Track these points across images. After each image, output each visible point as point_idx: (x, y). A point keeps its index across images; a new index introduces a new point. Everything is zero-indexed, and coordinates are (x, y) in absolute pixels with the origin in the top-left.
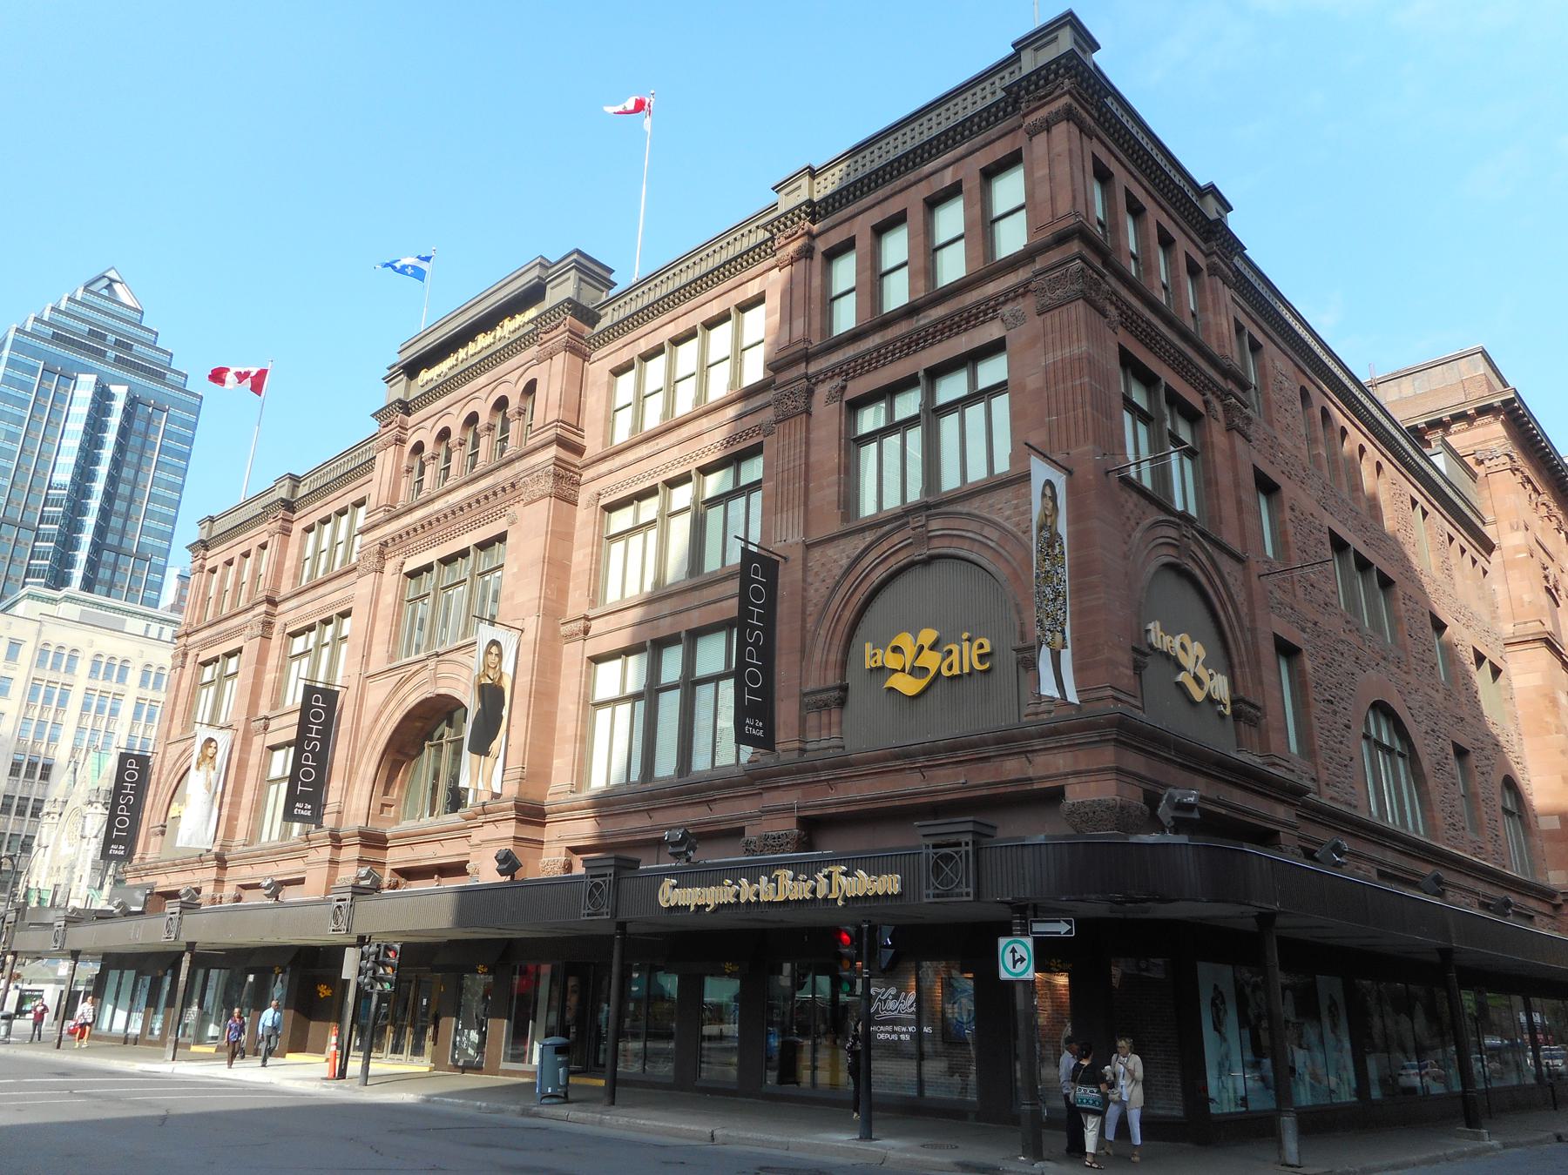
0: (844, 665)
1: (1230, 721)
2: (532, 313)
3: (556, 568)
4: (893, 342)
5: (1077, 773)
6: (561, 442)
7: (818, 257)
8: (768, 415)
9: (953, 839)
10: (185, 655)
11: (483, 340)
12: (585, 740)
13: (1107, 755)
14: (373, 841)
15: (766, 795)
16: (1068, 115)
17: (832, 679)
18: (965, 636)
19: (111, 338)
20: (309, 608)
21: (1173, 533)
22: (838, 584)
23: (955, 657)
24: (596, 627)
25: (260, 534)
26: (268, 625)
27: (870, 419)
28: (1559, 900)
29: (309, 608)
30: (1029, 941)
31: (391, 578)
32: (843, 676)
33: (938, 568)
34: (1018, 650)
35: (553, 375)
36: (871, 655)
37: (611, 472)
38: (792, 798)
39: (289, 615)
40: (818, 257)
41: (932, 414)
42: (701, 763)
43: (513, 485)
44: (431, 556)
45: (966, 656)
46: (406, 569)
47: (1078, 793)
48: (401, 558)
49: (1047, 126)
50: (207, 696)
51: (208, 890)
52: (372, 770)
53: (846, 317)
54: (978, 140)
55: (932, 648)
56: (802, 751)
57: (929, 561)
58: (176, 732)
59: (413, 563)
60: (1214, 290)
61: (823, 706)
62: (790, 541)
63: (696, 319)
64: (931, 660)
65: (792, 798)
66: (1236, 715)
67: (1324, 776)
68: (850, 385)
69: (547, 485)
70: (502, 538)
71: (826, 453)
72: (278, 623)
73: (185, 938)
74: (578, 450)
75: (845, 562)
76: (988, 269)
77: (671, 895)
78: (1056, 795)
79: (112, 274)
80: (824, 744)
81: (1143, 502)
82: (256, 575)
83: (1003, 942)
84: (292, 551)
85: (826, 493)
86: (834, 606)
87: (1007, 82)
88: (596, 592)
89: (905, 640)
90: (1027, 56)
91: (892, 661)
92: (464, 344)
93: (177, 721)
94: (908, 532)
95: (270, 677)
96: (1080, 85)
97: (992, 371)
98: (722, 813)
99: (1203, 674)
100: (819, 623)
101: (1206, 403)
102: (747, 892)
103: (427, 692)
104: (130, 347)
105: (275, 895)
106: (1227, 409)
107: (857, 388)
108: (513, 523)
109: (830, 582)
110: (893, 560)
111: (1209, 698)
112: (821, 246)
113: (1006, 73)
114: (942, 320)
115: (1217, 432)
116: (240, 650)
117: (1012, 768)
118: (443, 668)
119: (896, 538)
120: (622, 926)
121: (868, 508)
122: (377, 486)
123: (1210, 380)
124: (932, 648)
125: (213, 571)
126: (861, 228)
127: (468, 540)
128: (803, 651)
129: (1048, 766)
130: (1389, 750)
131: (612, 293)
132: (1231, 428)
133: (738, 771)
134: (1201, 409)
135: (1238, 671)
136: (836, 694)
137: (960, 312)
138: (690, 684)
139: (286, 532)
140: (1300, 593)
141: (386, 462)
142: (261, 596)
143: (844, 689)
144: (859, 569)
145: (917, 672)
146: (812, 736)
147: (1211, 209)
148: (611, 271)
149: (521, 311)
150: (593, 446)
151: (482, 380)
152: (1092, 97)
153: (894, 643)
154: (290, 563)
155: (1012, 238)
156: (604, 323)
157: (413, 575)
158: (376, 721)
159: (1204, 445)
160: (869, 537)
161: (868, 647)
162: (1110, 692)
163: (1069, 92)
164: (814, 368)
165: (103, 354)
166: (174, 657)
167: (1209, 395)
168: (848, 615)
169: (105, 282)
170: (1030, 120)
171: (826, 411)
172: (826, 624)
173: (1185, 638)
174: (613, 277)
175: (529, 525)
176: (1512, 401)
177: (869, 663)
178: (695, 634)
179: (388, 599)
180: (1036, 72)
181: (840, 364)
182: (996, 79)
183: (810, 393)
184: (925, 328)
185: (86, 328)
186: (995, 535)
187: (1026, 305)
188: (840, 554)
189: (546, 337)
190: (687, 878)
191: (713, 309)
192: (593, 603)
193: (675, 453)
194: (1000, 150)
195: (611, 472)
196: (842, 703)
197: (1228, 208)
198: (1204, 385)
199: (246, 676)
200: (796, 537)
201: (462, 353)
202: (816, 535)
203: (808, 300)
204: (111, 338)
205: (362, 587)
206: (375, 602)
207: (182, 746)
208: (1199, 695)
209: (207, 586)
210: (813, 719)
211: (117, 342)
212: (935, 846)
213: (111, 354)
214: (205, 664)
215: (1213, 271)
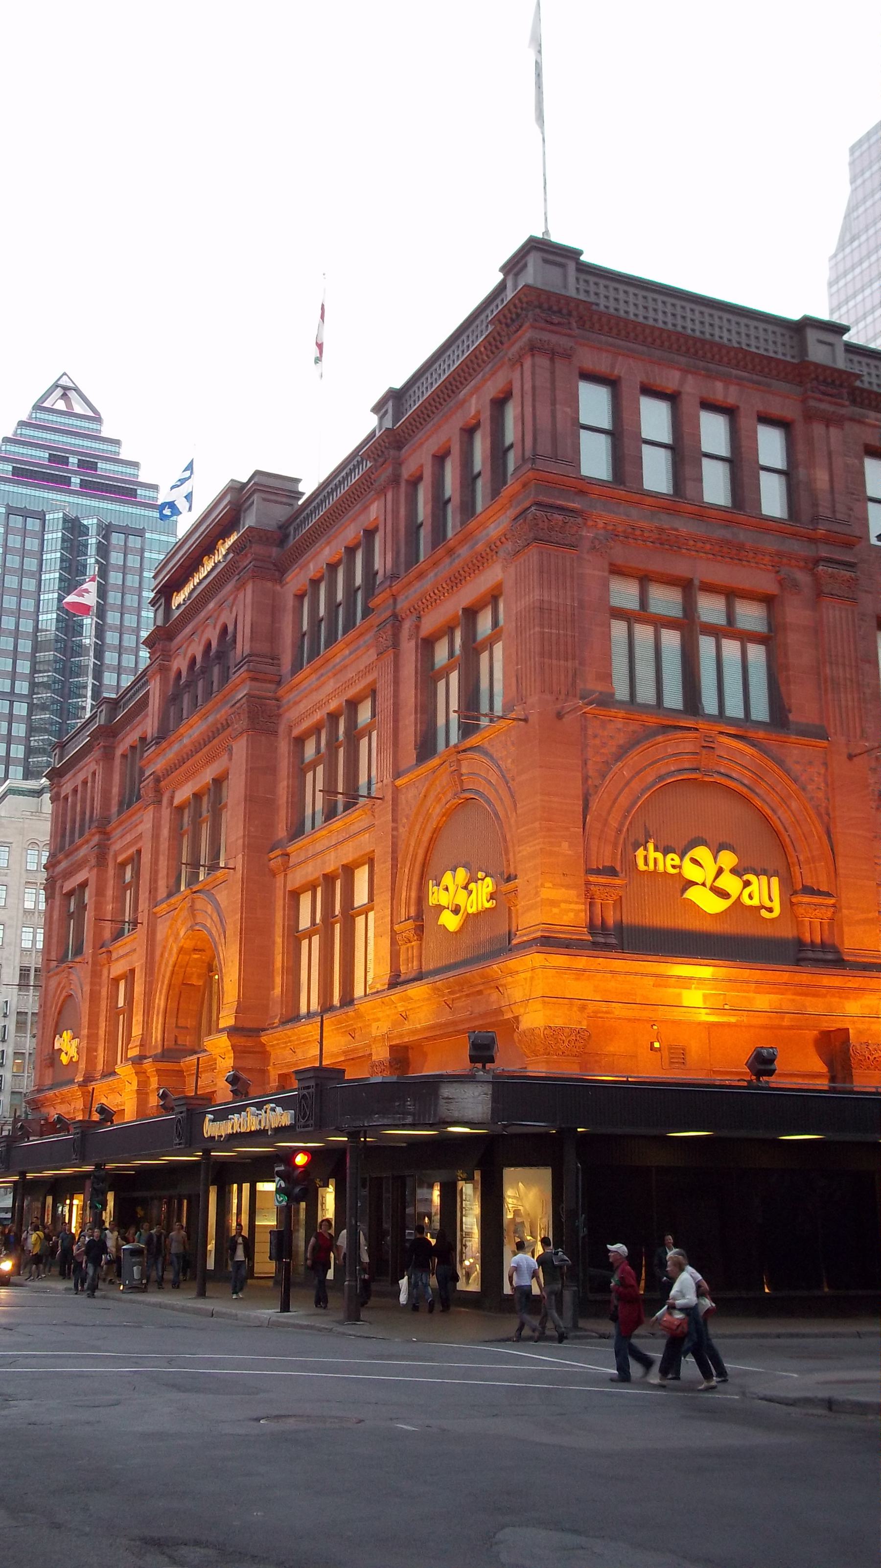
2: (234, 537)
16: (533, 349)
19: (74, 460)
46: (176, 802)
62: (385, 782)
69: (241, 724)
79: (64, 381)
104: (94, 466)
113: (493, 306)
128: (393, 890)
165: (67, 481)
169: (59, 392)
174: (301, 488)
204: (74, 460)
206: (156, 836)
213: (76, 480)
215: (809, 417)
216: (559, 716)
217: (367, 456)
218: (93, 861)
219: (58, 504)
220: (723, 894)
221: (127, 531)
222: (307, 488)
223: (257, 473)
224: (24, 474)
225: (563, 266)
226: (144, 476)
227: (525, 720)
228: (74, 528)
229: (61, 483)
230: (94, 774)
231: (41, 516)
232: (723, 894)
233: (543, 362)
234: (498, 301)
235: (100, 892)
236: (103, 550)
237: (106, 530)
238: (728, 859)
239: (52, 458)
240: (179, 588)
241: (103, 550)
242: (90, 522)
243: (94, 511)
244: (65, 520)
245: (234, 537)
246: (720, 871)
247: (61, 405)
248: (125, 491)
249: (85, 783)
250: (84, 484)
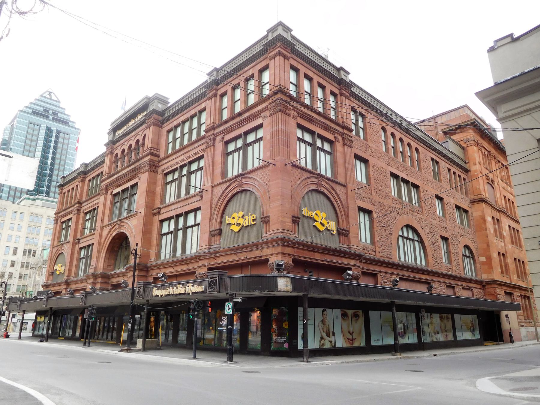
0: (221, 222)
1: (337, 236)
2: (145, 113)
3: (150, 193)
4: (235, 124)
5: (272, 254)
6: (151, 154)
7: (218, 96)
8: (204, 146)
9: (214, 276)
10: (57, 220)
11: (133, 122)
12: (159, 245)
13: (279, 249)
14: (106, 277)
15: (200, 262)
16: (280, 54)
17: (218, 228)
18: (250, 214)
19: (51, 112)
20: (90, 205)
21: (315, 180)
22: (220, 198)
23: (247, 220)
24: (162, 211)
25: (76, 183)
26: (79, 210)
28: (484, 284)
29: (90, 205)
30: (232, 304)
31: (109, 197)
32: (220, 226)
33: (245, 193)
34: (261, 218)
35: (150, 133)
36: (227, 219)
37: (166, 163)
38: (206, 262)
39: (86, 207)
40: (218, 96)
41: (246, 145)
42: (188, 252)
43: (139, 167)
44: (119, 189)
45: (249, 220)
46: (113, 193)
47: (273, 260)
48: (111, 190)
49: (274, 57)
50: (64, 232)
51: (64, 292)
52: (104, 255)
53: (225, 115)
54: (258, 61)
55: (242, 217)
56: (209, 248)
57: (243, 191)
58: (55, 244)
59: (115, 191)
60: (341, 101)
61: (215, 235)
63: (188, 115)
64: (241, 221)
65: (206, 262)
66: (339, 233)
67: (378, 249)
68: (225, 137)
69: (147, 168)
70: (137, 184)
71: (219, 158)
73: (49, 307)
74: (158, 156)
75: (222, 192)
76: (262, 100)
77: (156, 292)
78: (267, 261)
79: (50, 91)
80: (215, 246)
81: (303, 171)
82: (76, 194)
83: (226, 304)
84: (86, 187)
85: (218, 171)
86: (219, 205)
87: (264, 43)
88: (163, 200)
89: (235, 215)
90: (270, 35)
91: (232, 221)
92: (128, 123)
93: (56, 240)
94: (237, 183)
95: (80, 226)
96: (284, 43)
97: (260, 133)
98: (191, 266)
99: (324, 222)
100: (215, 210)
101: (335, 137)
103: (118, 231)
104: (57, 114)
105: (72, 294)
106: (343, 139)
108: (139, 179)
109: (218, 197)
110: (233, 191)
111: (327, 229)
112: (219, 93)
113: (263, 41)
114: (247, 118)
115: (339, 147)
116: (71, 219)
117: (257, 253)
118: (122, 224)
119: (234, 184)
120: (148, 301)
121: (230, 175)
122: (105, 169)
123: (336, 130)
124: (242, 217)
125: (65, 193)
127: (129, 184)
128: (210, 219)
129: (266, 252)
130: (413, 240)
131: (169, 105)
132: (344, 144)
133: (193, 255)
134: (333, 139)
135: (340, 220)
136: (218, 231)
137: (251, 115)
138: (186, 228)
139: (83, 181)
140: (374, 193)
141: (107, 160)
142: (76, 201)
143: (220, 230)
144: (225, 194)
145: (238, 224)
146: (213, 244)
147: (343, 75)
148: (168, 99)
149: (143, 112)
150: (162, 155)
151: (133, 134)
152: (289, 47)
153: (233, 216)
154: (85, 191)
156: (166, 115)
157: (115, 195)
158: (105, 240)
159: (334, 151)
160: (228, 184)
161: (227, 217)
162: (281, 231)
163: (280, 47)
164: (217, 131)
165: (48, 117)
166: (54, 220)
167: (336, 135)
168: (222, 207)
169: (48, 93)
170: (270, 55)
171: (219, 146)
172: (217, 210)
173: (318, 212)
174: (169, 101)
175: (143, 180)
176: (474, 122)
177: (227, 222)
178: (187, 213)
179: (108, 202)
180: (273, 39)
181: (222, 131)
182: (261, 43)
183: (214, 139)
184: (243, 120)
185: (42, 109)
186: (257, 183)
187: (267, 113)
188: (219, 190)
189: (148, 121)
190: (159, 288)
191: (193, 112)
192: (161, 204)
193: (182, 157)
194: (263, 64)
195: (166, 163)
196: (220, 234)
197: (348, 73)
198: (334, 132)
199: (73, 227)
200: (209, 184)
201: (127, 126)
202: (216, 183)
203: (215, 110)
204: (51, 112)
205: (102, 199)
206: (105, 204)
207: (57, 248)
208: (321, 228)
209: (63, 198)
210: (213, 238)
211: (53, 113)
212: (211, 278)
213: (51, 117)
214: (63, 223)
215: (341, 94)
216: (286, 165)
217: (205, 87)
218: (76, 212)
219: (44, 123)
220: (322, 224)
221: (65, 134)
222: (172, 101)
223: (156, 94)
224: (35, 113)
225: (287, 32)
226: (71, 119)
227: (275, 165)
228: (49, 130)
229: (47, 117)
230: (77, 186)
231: (40, 126)
232: (322, 224)
233: (282, 58)
234: (265, 39)
235: (77, 221)
236: (57, 137)
237: (58, 132)
238: (324, 215)
239: (44, 110)
240: (119, 129)
241: (57, 137)
242: (54, 129)
243: (55, 126)
244: (47, 127)
245: (145, 113)
246: (322, 218)
247: (48, 96)
248: (65, 122)
249: (73, 189)
250: (53, 118)
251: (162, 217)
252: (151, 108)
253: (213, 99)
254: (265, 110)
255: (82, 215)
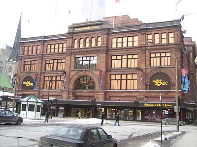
24: (112, 71)
26: (42, 58)
27: (153, 55)
49: (177, 31)
52: (73, 83)
64: (161, 83)
72: (44, 58)
89: (157, 80)
97: (169, 54)
102: (155, 105)
107: (151, 52)
126: (153, 33)
155: (172, 41)
251: (111, 73)
252: (104, 26)
253: (144, 35)
254: (174, 47)
255: (44, 61)
